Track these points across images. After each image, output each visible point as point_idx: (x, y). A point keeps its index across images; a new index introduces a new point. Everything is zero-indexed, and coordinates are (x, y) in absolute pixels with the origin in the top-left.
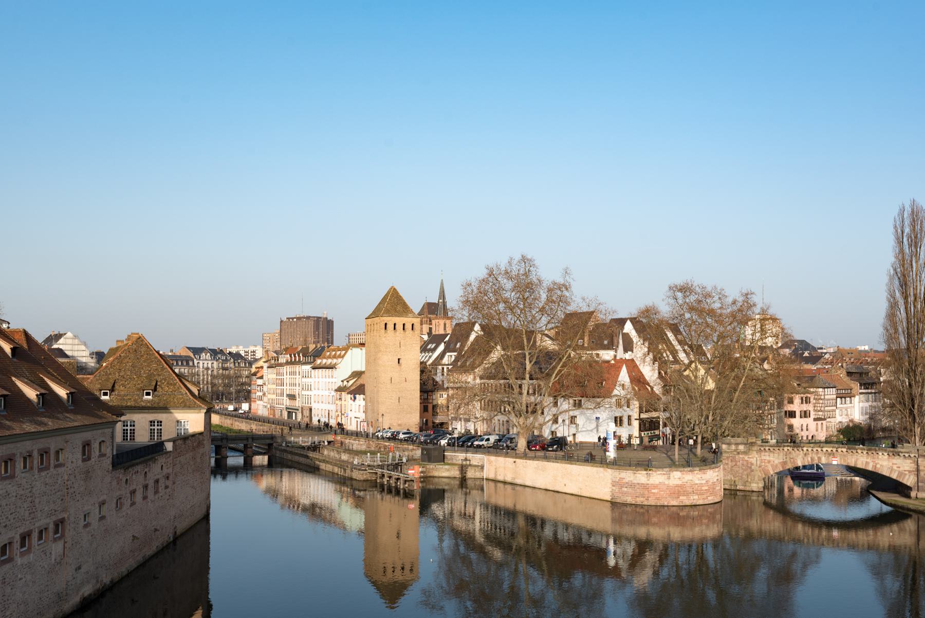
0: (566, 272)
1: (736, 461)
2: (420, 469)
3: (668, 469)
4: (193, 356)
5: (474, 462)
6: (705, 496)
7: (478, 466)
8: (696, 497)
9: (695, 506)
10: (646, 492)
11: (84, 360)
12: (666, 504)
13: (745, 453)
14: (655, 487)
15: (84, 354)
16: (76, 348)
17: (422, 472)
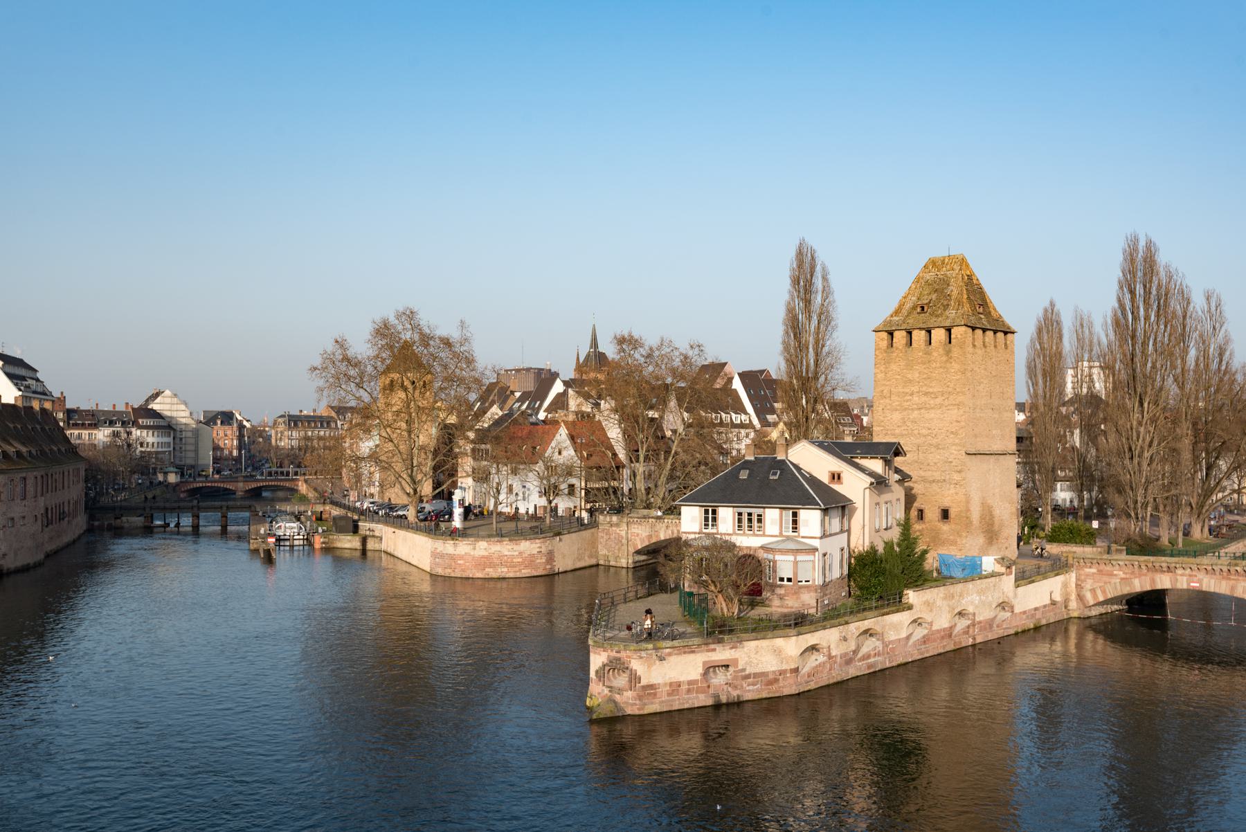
0: (462, 324)
1: (610, 535)
2: (322, 540)
3: (473, 539)
4: (336, 417)
5: (377, 534)
6: (517, 569)
7: (377, 537)
8: (506, 570)
9: (504, 578)
10: (453, 564)
11: (184, 421)
12: (471, 576)
13: (617, 525)
14: (461, 557)
15: (183, 414)
16: (175, 407)
17: (323, 543)
